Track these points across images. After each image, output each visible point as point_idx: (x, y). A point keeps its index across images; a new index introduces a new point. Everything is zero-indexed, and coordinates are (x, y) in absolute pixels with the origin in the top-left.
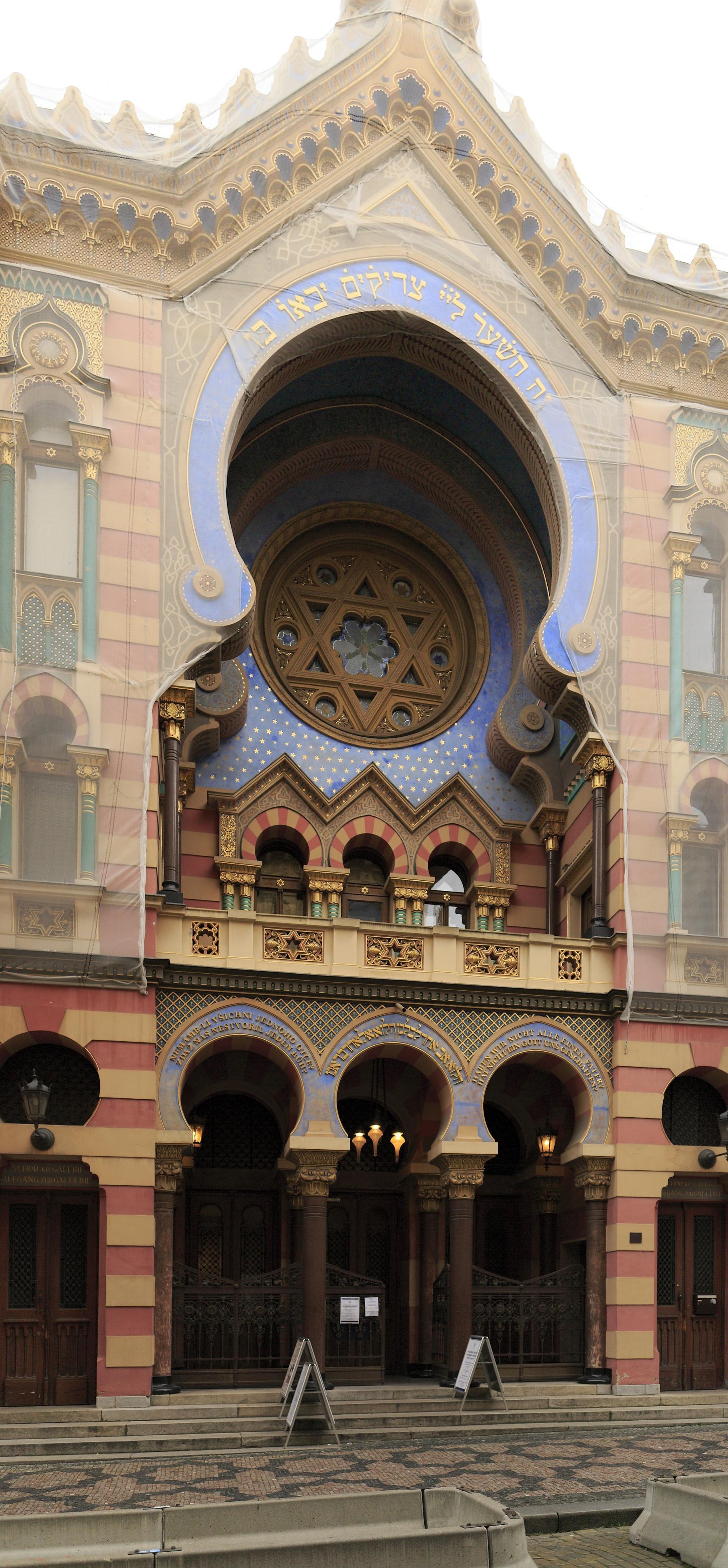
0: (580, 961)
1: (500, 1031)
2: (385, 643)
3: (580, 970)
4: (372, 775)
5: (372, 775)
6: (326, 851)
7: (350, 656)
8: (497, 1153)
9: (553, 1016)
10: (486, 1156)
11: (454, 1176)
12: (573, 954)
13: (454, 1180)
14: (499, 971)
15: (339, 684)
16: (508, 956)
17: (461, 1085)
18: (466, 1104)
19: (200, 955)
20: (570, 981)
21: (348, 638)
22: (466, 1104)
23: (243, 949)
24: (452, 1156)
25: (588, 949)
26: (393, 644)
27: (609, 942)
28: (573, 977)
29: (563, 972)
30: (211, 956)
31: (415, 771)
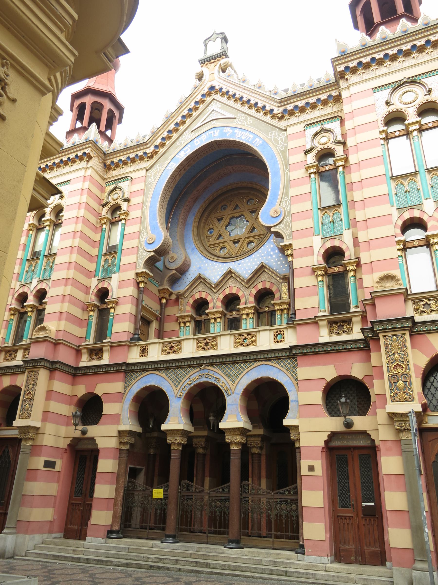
0: (284, 334)
1: (247, 370)
2: (245, 222)
3: (284, 338)
4: (230, 272)
5: (230, 272)
6: (216, 304)
7: (232, 231)
9: (269, 360)
10: (238, 429)
11: (228, 439)
12: (281, 331)
13: (227, 440)
15: (226, 241)
16: (252, 337)
17: (230, 397)
18: (232, 405)
19: (142, 357)
20: (279, 344)
21: (232, 225)
22: (232, 405)
23: (155, 353)
24: (225, 429)
25: (286, 328)
26: (247, 221)
27: (293, 324)
28: (281, 341)
29: (276, 340)
30: (145, 357)
31: (245, 267)
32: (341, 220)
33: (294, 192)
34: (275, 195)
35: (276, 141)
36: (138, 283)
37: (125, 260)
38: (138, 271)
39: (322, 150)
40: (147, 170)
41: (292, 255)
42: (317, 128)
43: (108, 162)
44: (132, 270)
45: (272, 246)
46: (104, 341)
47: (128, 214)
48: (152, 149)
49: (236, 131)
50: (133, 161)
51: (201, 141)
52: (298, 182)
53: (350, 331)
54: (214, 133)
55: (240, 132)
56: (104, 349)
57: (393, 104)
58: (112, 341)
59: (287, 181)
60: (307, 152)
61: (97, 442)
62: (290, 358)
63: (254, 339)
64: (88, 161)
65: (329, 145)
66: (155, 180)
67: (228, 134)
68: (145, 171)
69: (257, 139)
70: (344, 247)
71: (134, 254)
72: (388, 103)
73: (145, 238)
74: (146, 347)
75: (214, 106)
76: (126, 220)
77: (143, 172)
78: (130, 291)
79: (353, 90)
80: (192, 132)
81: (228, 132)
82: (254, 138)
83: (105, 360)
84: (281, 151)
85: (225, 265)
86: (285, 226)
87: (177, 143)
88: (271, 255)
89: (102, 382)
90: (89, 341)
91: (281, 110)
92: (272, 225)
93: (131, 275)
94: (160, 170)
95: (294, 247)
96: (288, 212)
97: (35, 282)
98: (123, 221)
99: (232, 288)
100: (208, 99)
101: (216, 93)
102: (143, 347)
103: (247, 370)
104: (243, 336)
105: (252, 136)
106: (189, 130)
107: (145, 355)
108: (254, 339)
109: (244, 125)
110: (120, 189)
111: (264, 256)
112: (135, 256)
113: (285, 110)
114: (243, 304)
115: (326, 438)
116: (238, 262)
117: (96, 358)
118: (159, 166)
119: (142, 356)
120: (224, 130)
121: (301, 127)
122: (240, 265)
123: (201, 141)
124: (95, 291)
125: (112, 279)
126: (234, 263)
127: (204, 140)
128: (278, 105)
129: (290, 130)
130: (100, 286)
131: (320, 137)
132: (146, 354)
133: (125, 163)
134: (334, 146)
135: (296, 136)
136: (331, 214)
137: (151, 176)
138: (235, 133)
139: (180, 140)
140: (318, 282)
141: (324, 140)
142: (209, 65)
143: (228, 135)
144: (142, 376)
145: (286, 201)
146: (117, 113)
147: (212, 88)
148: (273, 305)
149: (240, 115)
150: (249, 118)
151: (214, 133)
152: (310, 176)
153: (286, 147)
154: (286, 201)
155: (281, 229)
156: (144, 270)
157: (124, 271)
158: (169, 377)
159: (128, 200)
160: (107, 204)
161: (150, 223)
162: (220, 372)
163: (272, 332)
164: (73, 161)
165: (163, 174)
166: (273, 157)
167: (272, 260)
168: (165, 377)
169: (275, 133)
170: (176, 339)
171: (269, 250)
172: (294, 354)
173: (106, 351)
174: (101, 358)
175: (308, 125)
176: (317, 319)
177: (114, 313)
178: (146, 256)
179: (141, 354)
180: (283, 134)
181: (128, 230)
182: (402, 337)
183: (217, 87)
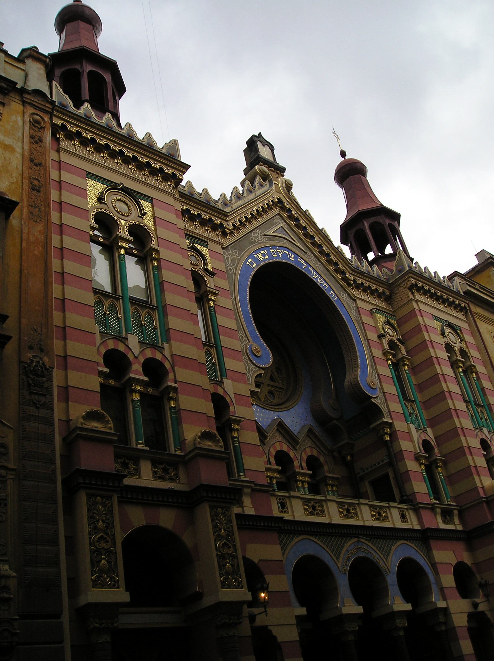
8: (411, 609)
32: (416, 416)
53: (451, 522)
61: (274, 633)
67: (304, 267)
74: (283, 500)
91: (352, 278)
93: (245, 389)
101: (283, 208)
106: (258, 231)
115: (466, 619)
121: (369, 307)
134: (398, 343)
136: (409, 406)
140: (422, 470)
144: (295, 540)
148: (326, 478)
170: (318, 498)
172: (425, 537)
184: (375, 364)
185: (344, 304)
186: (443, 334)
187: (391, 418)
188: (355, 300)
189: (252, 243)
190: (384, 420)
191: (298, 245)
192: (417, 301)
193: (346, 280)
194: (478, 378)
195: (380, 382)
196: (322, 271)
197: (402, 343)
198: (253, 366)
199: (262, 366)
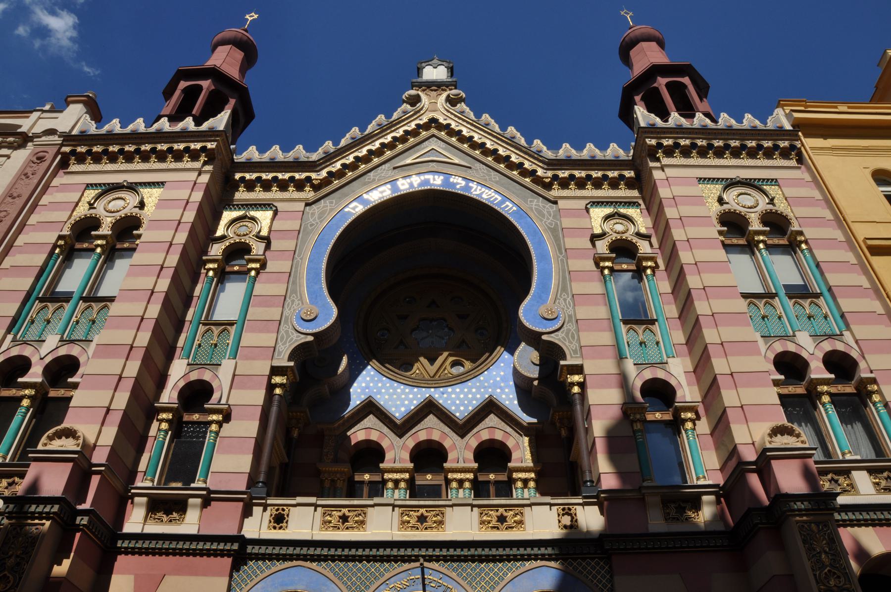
2: (446, 330)
12: (570, 509)
14: (510, 528)
19: (273, 531)
26: (451, 329)
30: (281, 531)
32: (658, 343)
33: (577, 288)
34: (545, 287)
35: (540, 212)
36: (271, 387)
37: (248, 339)
38: (276, 363)
39: (617, 240)
40: (307, 205)
41: (582, 385)
42: (608, 210)
43: (238, 176)
44: (264, 359)
45: (502, 373)
46: (193, 485)
47: (264, 265)
48: (324, 173)
49: (471, 184)
50: (283, 186)
51: (411, 185)
52: (582, 275)
54: (434, 179)
55: (479, 188)
56: (191, 501)
57: (727, 203)
58: (212, 488)
59: (564, 271)
60: (594, 238)
62: (595, 558)
63: (518, 518)
64: (205, 163)
65: (629, 236)
66: (321, 222)
68: (304, 204)
69: (508, 203)
70: (673, 382)
71: (272, 332)
72: (721, 201)
73: (294, 309)
75: (433, 144)
76: (258, 273)
77: (301, 206)
78: (258, 397)
79: (669, 172)
80: (395, 168)
81: (458, 184)
82: (502, 202)
83: (191, 523)
84: (549, 228)
85: (416, 390)
86: (567, 334)
87: (366, 177)
88: (500, 388)
89: (178, 572)
90: (153, 481)
91: (550, 174)
92: (544, 330)
94: (331, 210)
95: (587, 370)
96: (570, 316)
97: (52, 341)
98: (253, 273)
99: (431, 429)
100: (424, 134)
102: (277, 510)
103: (510, 576)
104: (497, 511)
105: (499, 198)
107: (280, 528)
108: (518, 518)
109: (486, 180)
110: (253, 219)
111: (490, 387)
112: (274, 335)
113: (555, 177)
114: (453, 461)
116: (441, 389)
117: (165, 518)
118: (332, 203)
119: (275, 528)
120: (451, 180)
121: (582, 204)
122: (445, 396)
123: (411, 185)
124: (182, 384)
125: (221, 369)
126: (432, 390)
127: (416, 185)
128: (545, 167)
129: (561, 203)
130: (194, 376)
131: (612, 222)
132: (284, 524)
133: (267, 186)
134: (635, 240)
135: (572, 213)
136: (640, 331)
137: (313, 214)
138: (471, 188)
139: (372, 174)
140: (634, 432)
141: (619, 228)
142: (428, 92)
143: (458, 187)
145: (565, 300)
146: (242, 120)
147: (433, 120)
149: (478, 165)
150: (493, 173)
151: (434, 179)
152: (602, 272)
153: (556, 224)
154: (565, 300)
155: (559, 340)
156: (292, 364)
157: (246, 358)
158: (341, 579)
159: (267, 240)
160: (223, 238)
161: (307, 287)
162: (454, 575)
163: (555, 508)
164: (178, 156)
165: (338, 216)
166: (536, 233)
167: (504, 396)
168: (331, 575)
169: (538, 202)
171: (498, 379)
173: (194, 506)
174: (181, 520)
175: (594, 203)
176: (643, 491)
177: (217, 433)
178: (296, 341)
179: (272, 524)
180: (552, 208)
181: (260, 288)
182: (825, 526)
183: (441, 121)
184: (571, 281)
185: (529, 213)
186: (721, 201)
187: (582, 356)
188: (555, 203)
189: (365, 184)
190: (562, 363)
191: (456, 161)
192: (662, 168)
193: (538, 181)
194: (810, 250)
195: (574, 305)
196: (497, 182)
197: (646, 237)
198: (296, 334)
199: (308, 331)
